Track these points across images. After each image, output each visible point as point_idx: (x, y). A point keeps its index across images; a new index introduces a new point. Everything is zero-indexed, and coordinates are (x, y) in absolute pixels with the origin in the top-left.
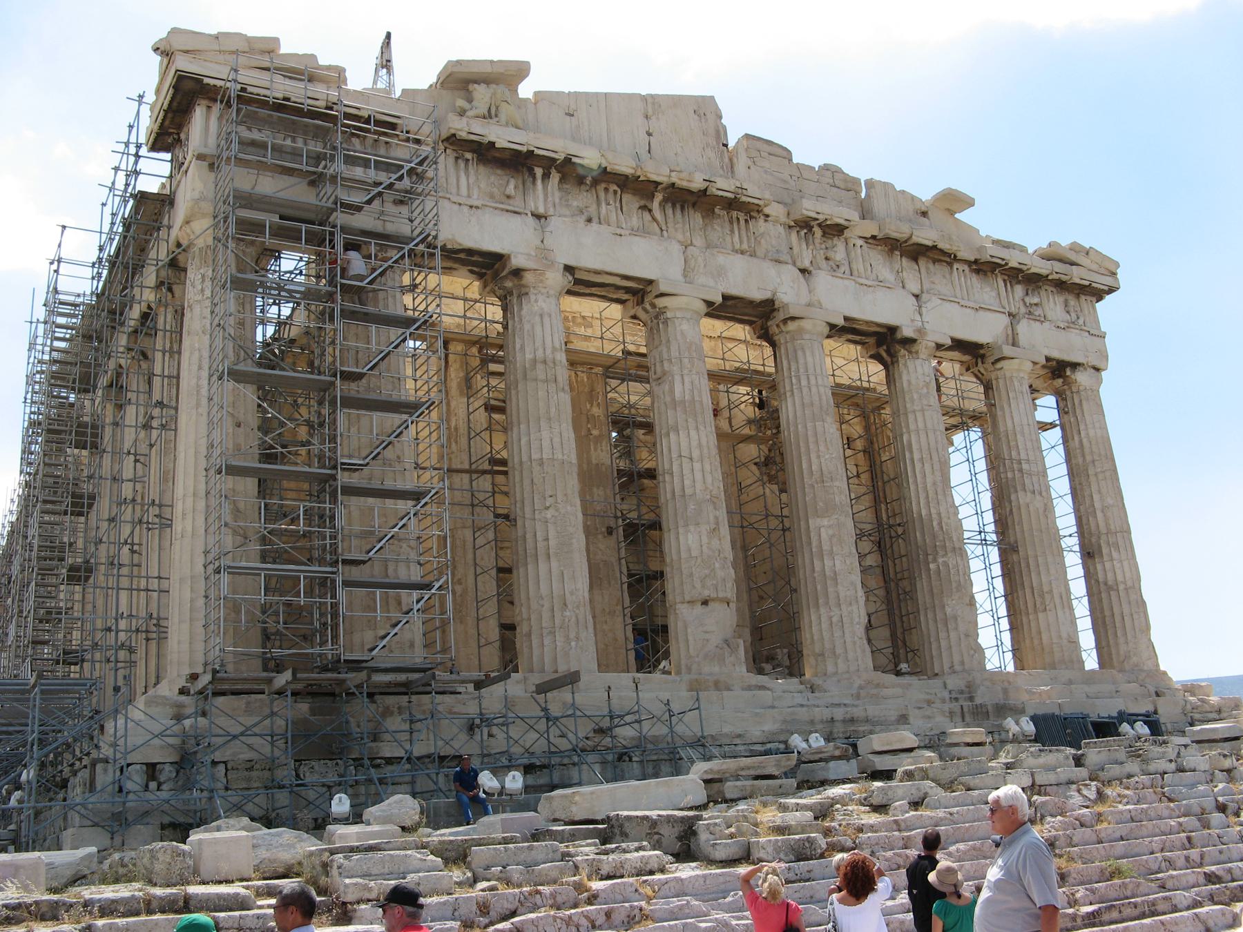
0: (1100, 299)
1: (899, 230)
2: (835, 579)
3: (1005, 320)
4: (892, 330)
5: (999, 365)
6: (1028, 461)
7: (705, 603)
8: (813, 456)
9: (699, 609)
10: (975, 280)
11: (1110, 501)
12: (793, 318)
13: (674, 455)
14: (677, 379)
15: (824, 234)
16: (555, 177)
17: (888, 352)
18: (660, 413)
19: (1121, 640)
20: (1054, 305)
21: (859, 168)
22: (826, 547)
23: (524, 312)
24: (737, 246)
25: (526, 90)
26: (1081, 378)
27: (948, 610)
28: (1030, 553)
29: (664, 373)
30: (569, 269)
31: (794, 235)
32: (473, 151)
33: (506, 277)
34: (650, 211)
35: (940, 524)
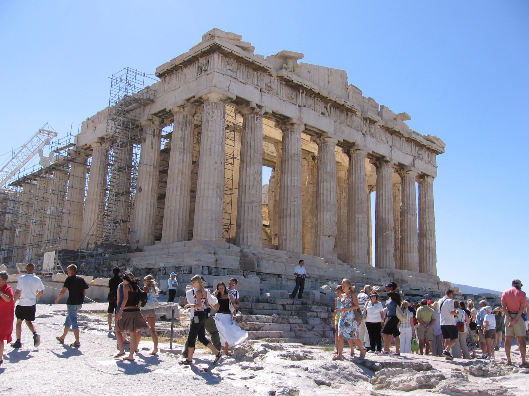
0: (437, 154)
1: (390, 125)
2: (361, 234)
3: (412, 158)
4: (383, 157)
5: (408, 172)
6: (412, 205)
7: (329, 236)
8: (359, 195)
9: (327, 238)
10: (406, 144)
11: (431, 221)
12: (359, 150)
13: (325, 189)
14: (329, 164)
15: (370, 123)
16: (305, 93)
17: (380, 163)
18: (321, 175)
19: (428, 265)
20: (425, 154)
21: (380, 102)
22: (360, 224)
23: (292, 137)
24: (348, 124)
25: (299, 62)
26: (429, 180)
27: (387, 248)
28: (409, 234)
29: (324, 162)
30: (305, 125)
31: (362, 122)
32: (285, 81)
33: (288, 125)
34: (327, 108)
35: (388, 221)
